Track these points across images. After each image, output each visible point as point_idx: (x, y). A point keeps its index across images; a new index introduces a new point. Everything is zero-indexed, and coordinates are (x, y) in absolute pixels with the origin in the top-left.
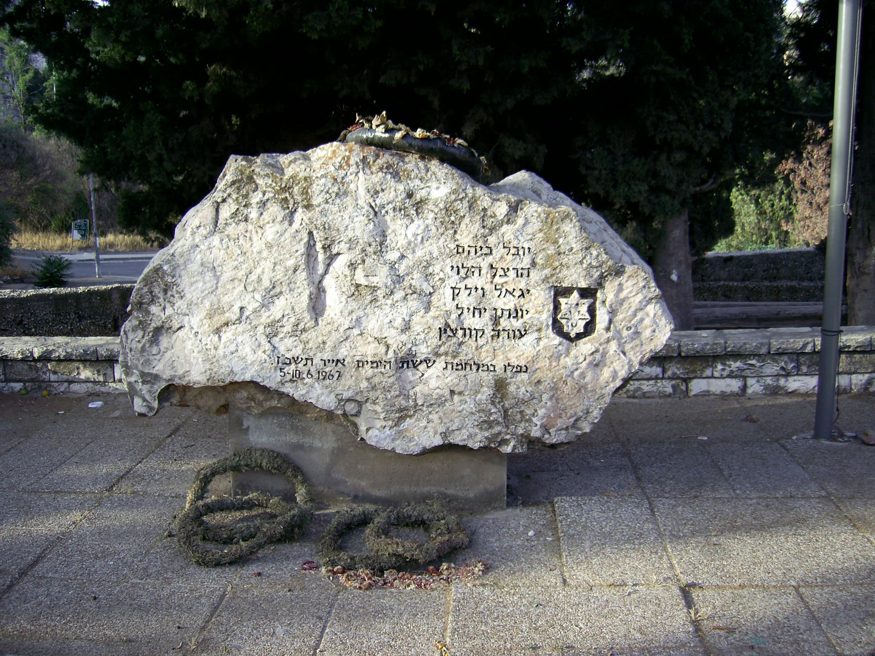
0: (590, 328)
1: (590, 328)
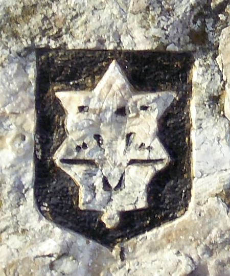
0: (169, 190)
1: (169, 190)
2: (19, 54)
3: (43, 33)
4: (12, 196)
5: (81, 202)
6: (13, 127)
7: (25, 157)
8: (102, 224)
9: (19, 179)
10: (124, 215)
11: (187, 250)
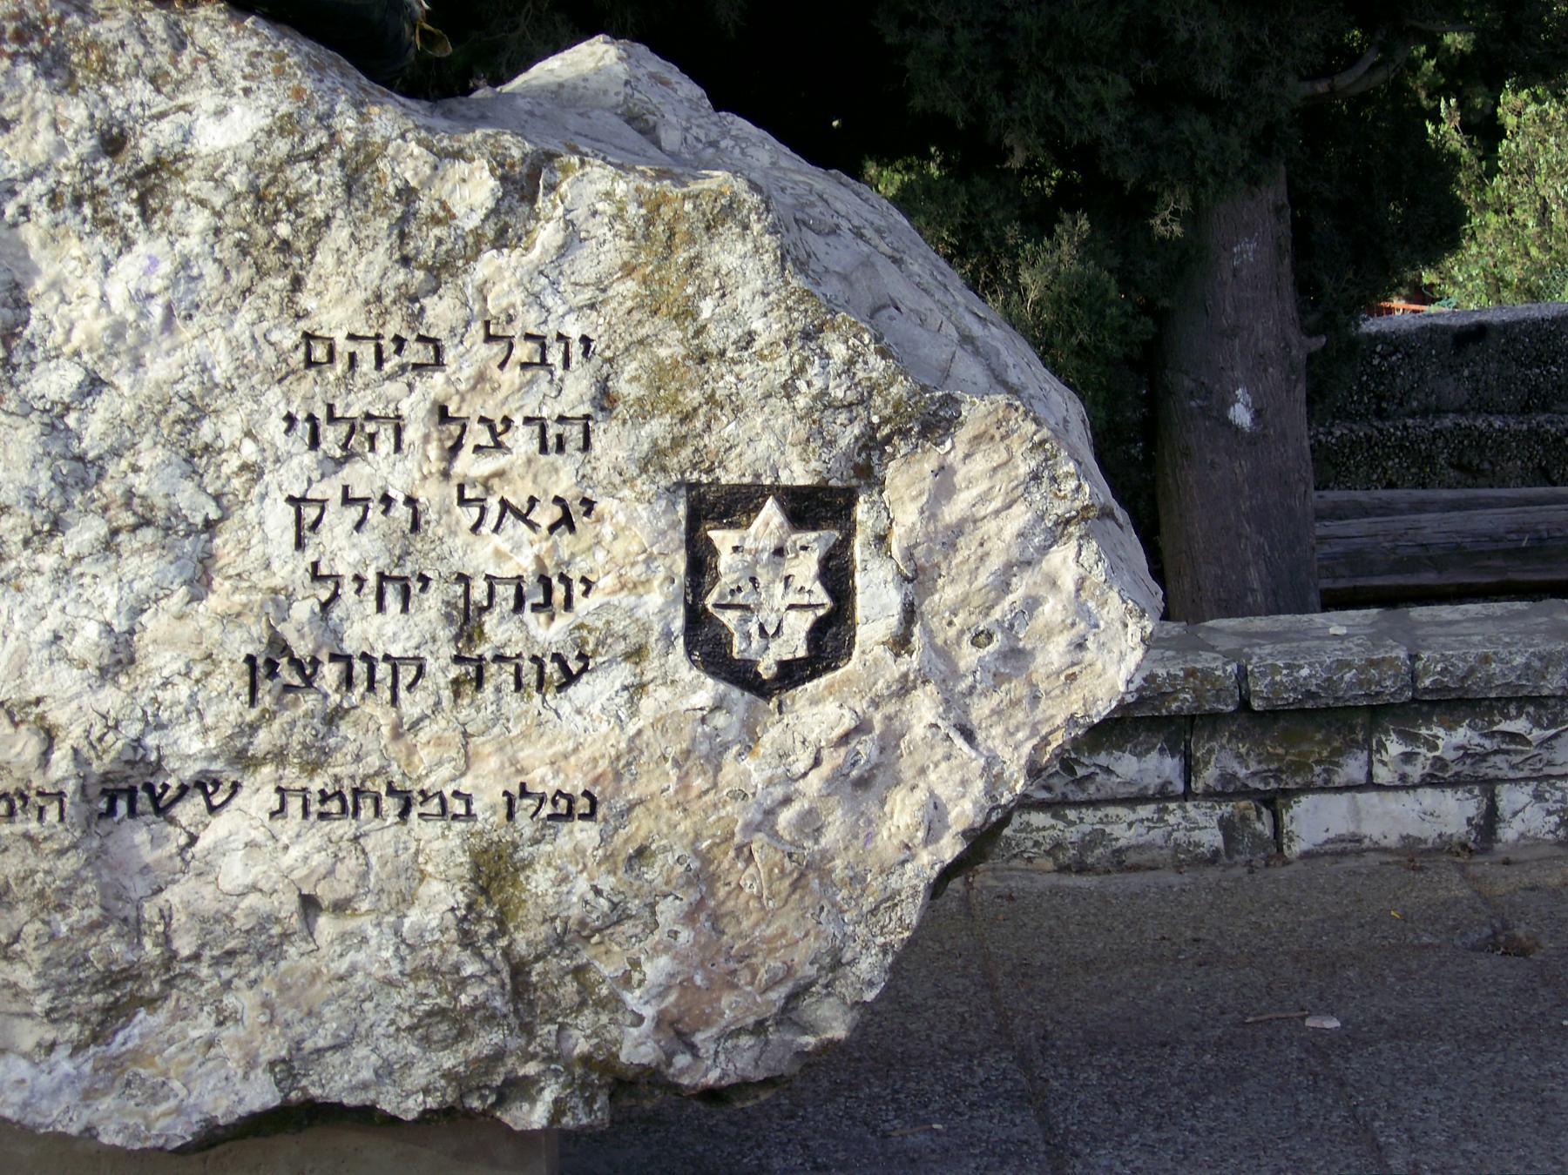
0: (830, 639)
1: (830, 639)
2: (668, 489)
3: (694, 466)
4: (660, 644)
5: (735, 650)
6: (661, 568)
7: (674, 601)
8: (758, 675)
9: (668, 625)
10: (784, 666)
11: (851, 702)
